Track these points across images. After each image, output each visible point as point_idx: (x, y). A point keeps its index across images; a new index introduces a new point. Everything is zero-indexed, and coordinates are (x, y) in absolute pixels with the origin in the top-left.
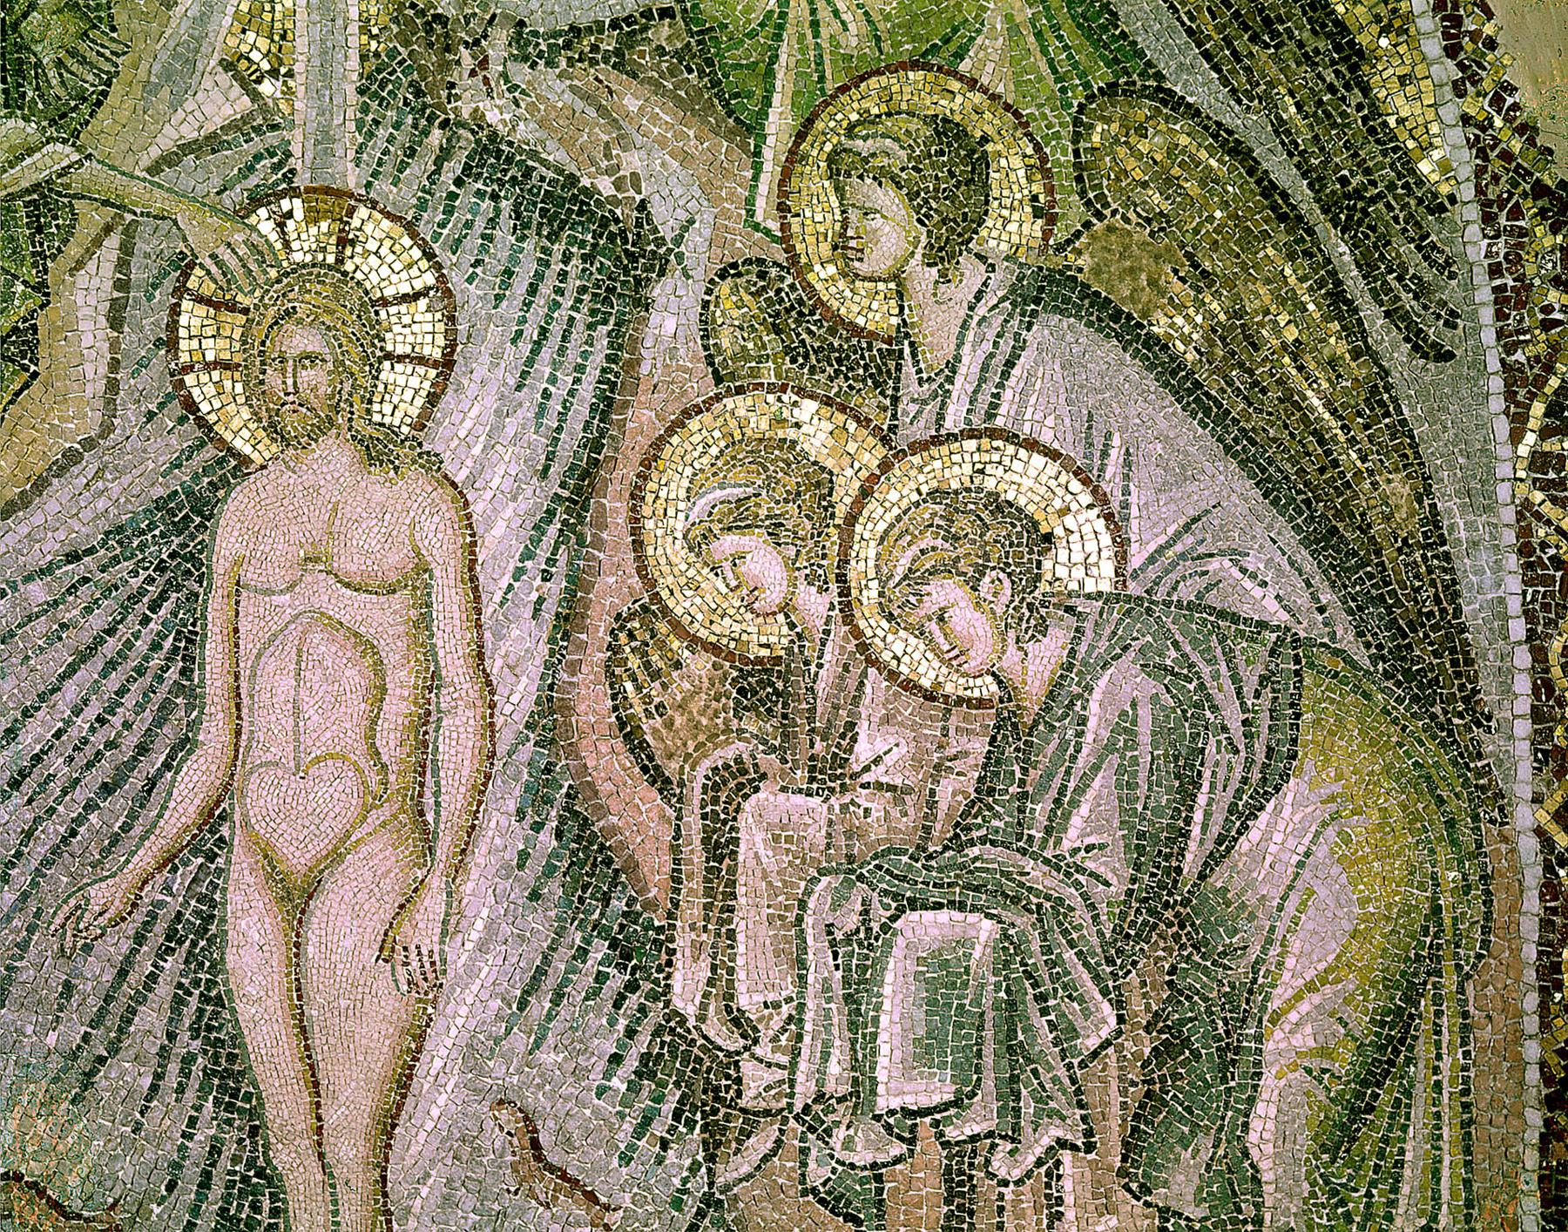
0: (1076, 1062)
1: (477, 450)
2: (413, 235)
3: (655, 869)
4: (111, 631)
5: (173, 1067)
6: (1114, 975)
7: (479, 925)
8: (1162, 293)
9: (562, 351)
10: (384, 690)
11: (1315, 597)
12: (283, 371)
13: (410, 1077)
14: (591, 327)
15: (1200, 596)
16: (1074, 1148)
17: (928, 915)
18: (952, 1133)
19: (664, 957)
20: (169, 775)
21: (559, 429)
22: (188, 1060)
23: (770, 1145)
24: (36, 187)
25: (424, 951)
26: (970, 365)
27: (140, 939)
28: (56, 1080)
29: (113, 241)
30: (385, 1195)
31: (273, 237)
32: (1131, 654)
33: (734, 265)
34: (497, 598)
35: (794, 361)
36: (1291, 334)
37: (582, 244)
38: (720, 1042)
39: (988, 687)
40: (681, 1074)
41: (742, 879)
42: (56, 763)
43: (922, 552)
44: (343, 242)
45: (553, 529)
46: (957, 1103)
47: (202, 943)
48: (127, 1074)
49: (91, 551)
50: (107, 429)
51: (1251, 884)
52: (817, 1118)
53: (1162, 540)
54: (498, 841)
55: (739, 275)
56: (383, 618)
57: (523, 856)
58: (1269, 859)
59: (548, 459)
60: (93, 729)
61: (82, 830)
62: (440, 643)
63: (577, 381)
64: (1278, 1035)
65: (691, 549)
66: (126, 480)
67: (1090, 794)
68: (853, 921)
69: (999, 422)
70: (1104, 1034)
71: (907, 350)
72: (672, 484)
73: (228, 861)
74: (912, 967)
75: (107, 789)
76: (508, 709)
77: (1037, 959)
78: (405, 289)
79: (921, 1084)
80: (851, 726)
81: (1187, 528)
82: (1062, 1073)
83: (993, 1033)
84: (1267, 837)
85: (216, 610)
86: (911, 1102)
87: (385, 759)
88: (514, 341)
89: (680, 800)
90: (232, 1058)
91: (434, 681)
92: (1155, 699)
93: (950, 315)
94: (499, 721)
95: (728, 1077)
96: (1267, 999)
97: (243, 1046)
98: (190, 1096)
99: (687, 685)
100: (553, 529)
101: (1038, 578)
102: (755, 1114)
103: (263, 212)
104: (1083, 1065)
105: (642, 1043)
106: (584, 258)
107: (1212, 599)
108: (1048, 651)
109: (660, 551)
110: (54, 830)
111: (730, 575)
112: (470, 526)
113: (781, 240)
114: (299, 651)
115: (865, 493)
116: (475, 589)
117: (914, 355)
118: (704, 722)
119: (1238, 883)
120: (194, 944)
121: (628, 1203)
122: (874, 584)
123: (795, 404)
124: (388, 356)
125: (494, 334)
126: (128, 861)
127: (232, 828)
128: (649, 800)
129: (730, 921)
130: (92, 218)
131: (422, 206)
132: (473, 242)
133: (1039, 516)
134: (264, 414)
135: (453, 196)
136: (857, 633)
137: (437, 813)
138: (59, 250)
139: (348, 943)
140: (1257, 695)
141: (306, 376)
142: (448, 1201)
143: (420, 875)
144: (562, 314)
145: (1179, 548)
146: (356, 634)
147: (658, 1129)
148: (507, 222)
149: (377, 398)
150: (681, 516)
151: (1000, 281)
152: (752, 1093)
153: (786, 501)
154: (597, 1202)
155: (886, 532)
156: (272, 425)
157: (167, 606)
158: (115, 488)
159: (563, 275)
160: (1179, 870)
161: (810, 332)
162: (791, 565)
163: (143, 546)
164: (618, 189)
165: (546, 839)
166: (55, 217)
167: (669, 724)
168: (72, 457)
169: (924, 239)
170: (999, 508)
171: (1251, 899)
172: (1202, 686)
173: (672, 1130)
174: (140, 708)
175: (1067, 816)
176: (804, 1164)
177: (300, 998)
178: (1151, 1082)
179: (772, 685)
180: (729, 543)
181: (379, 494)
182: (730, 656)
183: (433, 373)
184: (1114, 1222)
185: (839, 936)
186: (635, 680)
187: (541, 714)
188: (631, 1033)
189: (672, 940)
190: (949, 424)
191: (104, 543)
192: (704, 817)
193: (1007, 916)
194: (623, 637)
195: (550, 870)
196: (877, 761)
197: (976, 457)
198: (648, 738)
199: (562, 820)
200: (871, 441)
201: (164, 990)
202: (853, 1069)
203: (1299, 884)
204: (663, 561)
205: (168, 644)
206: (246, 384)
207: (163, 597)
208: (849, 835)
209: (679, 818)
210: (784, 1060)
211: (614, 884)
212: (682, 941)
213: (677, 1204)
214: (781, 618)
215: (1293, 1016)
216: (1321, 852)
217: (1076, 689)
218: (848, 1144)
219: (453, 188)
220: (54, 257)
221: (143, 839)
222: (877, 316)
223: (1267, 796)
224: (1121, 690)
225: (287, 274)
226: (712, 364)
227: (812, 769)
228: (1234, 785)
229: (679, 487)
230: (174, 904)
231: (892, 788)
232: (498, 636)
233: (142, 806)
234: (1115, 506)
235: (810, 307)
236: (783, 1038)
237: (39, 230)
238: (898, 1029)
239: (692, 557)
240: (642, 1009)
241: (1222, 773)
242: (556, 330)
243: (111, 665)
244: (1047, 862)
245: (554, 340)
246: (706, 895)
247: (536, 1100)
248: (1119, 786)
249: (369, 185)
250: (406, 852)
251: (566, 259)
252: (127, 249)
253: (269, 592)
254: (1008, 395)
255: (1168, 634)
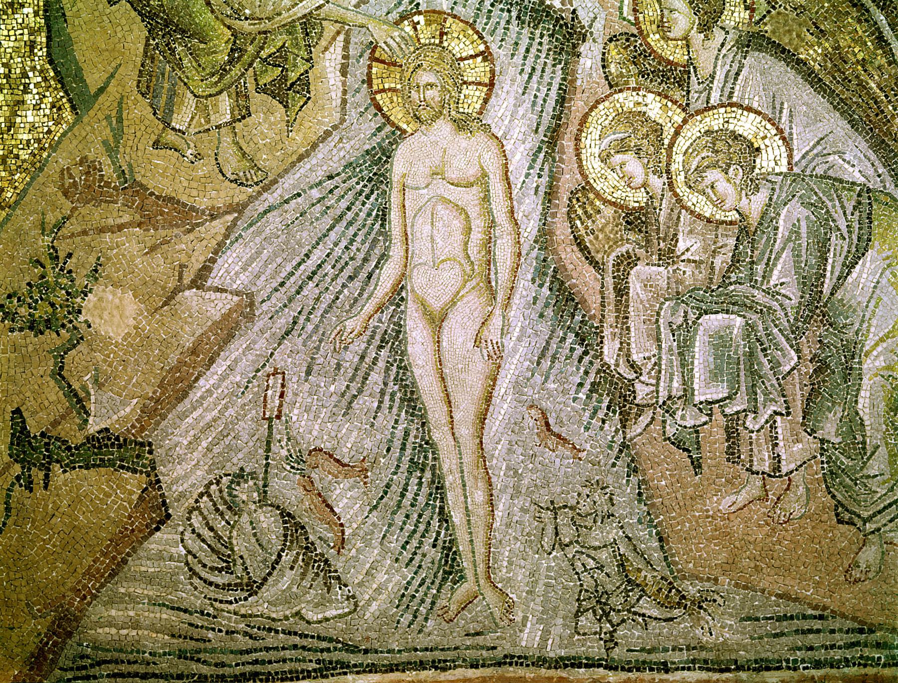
0: (780, 377)
1: (506, 122)
2: (474, 29)
3: (594, 302)
4: (349, 209)
5: (387, 398)
6: (795, 338)
7: (518, 329)
8: (803, 40)
9: (541, 77)
10: (470, 229)
11: (876, 171)
12: (419, 92)
13: (491, 397)
14: (554, 66)
15: (825, 172)
16: (782, 414)
17: (713, 316)
18: (728, 411)
19: (599, 340)
20: (378, 271)
21: (542, 111)
22: (393, 395)
23: (649, 419)
24: (305, 16)
25: (494, 342)
26: (720, 75)
27: (369, 343)
28: (335, 406)
29: (341, 37)
30: (482, 449)
31: (412, 33)
32: (796, 198)
33: (615, 36)
34: (519, 186)
35: (643, 77)
36: (860, 56)
37: (549, 29)
38: (625, 375)
39: (734, 216)
40: (609, 390)
41: (632, 304)
42: (328, 268)
43: (703, 158)
44: (442, 34)
45: (542, 155)
46: (728, 398)
47: (397, 343)
48: (367, 402)
49: (338, 174)
50: (343, 121)
51: (854, 296)
52: (669, 406)
53: (808, 148)
54: (524, 293)
55: (618, 40)
56: (469, 198)
57: (535, 299)
58: (861, 286)
59: (538, 124)
60: (343, 253)
61: (341, 296)
62: (494, 207)
63: (549, 90)
64: (869, 361)
65: (602, 161)
66: (352, 142)
67: (781, 260)
68: (681, 320)
69: (734, 99)
70: (792, 364)
71: (692, 70)
72: (592, 134)
73: (406, 307)
74: (706, 339)
75: (351, 278)
76: (526, 235)
77: (761, 333)
78: (472, 53)
79: (713, 390)
80: (675, 235)
81: (818, 143)
82: (775, 382)
83: (745, 367)
84: (860, 276)
85: (395, 199)
86: (709, 397)
87: (472, 259)
88: (520, 74)
89: (603, 271)
90: (412, 392)
91: (492, 224)
92: (807, 218)
93: (710, 54)
94: (522, 240)
95: (629, 390)
96: (862, 346)
97: (417, 387)
98: (395, 410)
99: (603, 221)
100: (542, 155)
101: (754, 167)
102: (644, 406)
103: (406, 22)
104: (784, 378)
105: (592, 378)
106: (552, 36)
107: (831, 173)
108: (760, 199)
109: (589, 162)
110: (329, 297)
111: (619, 172)
112: (505, 156)
113: (635, 25)
114: (433, 214)
115: (677, 133)
116: (509, 184)
117: (695, 72)
118: (612, 236)
119: (848, 296)
120: (393, 343)
121: (588, 448)
122: (682, 173)
123: (644, 96)
124: (465, 83)
125: (512, 71)
126: (361, 310)
127: (407, 293)
128: (589, 272)
129: (626, 323)
130: (330, 29)
131: (477, 16)
132: (500, 31)
133: (753, 140)
134: (411, 111)
135: (490, 11)
136: (676, 195)
137: (497, 282)
138: (317, 43)
139: (461, 340)
140: (852, 215)
141: (430, 93)
142: (510, 451)
143: (490, 309)
144: (542, 60)
145: (815, 151)
146: (457, 206)
147: (601, 415)
148: (515, 22)
149: (461, 102)
150: (597, 147)
151: (732, 36)
152: (640, 397)
153: (642, 139)
154: (575, 448)
155: (687, 150)
156: (415, 115)
157: (373, 197)
158: (348, 146)
159: (540, 44)
160: (821, 292)
161: (649, 64)
162: (646, 166)
163: (361, 171)
164: (563, 5)
165: (545, 291)
166: (314, 29)
167: (597, 238)
168: (328, 134)
169: (697, 22)
170: (736, 138)
171: (853, 302)
172: (828, 212)
173: (606, 415)
174: (363, 242)
175: (772, 270)
176: (664, 427)
177: (441, 365)
178: (814, 384)
179: (640, 219)
180: (618, 158)
181: (464, 144)
182: (621, 207)
183: (485, 89)
184: (800, 446)
185: (675, 327)
186: (580, 219)
187: (541, 236)
188: (586, 373)
189: (602, 332)
190: (712, 101)
191: (343, 171)
192: (614, 278)
193: (748, 315)
194: (574, 201)
195: (546, 305)
196: (688, 250)
197: (725, 115)
198: (588, 244)
199: (552, 282)
200: (679, 110)
201: (381, 364)
202: (684, 384)
203: (875, 296)
204: (590, 167)
205: (374, 213)
206: (403, 98)
207: (372, 192)
208: (677, 282)
209: (603, 279)
210: (654, 382)
211: (575, 309)
212: (607, 332)
213: (610, 447)
214: (643, 189)
215: (875, 353)
216: (884, 281)
217: (773, 215)
218: (683, 417)
219: (490, 8)
220: (314, 47)
221: (368, 299)
222: (678, 56)
223: (859, 258)
224: (793, 215)
225: (418, 49)
226: (607, 80)
227: (660, 255)
228: (844, 254)
229: (596, 135)
230: (383, 327)
231: (694, 261)
232: (520, 203)
233: (367, 285)
234: (786, 135)
235: (648, 53)
236: (653, 372)
237: (307, 34)
238: (702, 366)
239: (603, 165)
240: (591, 363)
241: (838, 248)
242: (539, 68)
243: (350, 224)
244: (764, 291)
245: (538, 72)
246: (616, 312)
247: (546, 404)
248: (793, 256)
249: (452, 8)
250: (483, 300)
251: (542, 36)
252: (347, 41)
253: (417, 188)
254: (737, 88)
255: (812, 190)
